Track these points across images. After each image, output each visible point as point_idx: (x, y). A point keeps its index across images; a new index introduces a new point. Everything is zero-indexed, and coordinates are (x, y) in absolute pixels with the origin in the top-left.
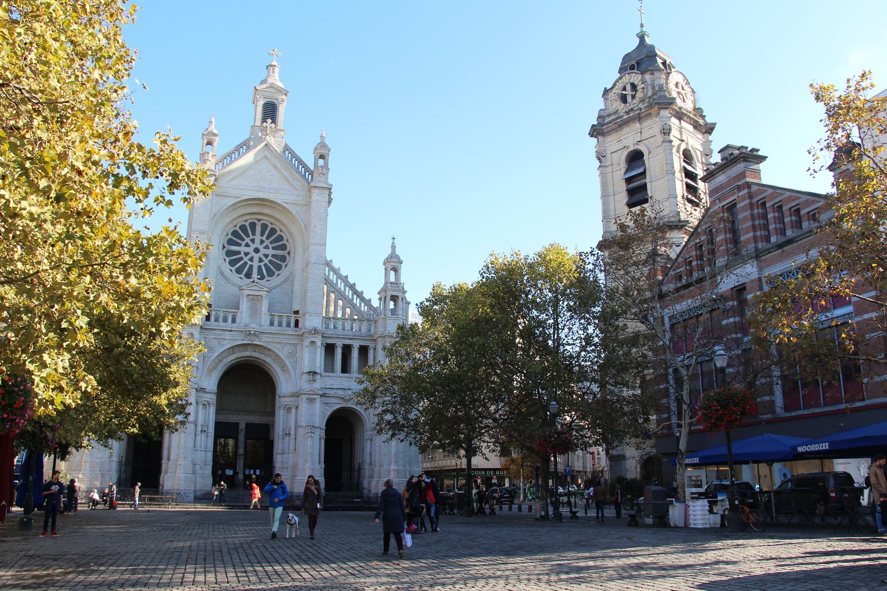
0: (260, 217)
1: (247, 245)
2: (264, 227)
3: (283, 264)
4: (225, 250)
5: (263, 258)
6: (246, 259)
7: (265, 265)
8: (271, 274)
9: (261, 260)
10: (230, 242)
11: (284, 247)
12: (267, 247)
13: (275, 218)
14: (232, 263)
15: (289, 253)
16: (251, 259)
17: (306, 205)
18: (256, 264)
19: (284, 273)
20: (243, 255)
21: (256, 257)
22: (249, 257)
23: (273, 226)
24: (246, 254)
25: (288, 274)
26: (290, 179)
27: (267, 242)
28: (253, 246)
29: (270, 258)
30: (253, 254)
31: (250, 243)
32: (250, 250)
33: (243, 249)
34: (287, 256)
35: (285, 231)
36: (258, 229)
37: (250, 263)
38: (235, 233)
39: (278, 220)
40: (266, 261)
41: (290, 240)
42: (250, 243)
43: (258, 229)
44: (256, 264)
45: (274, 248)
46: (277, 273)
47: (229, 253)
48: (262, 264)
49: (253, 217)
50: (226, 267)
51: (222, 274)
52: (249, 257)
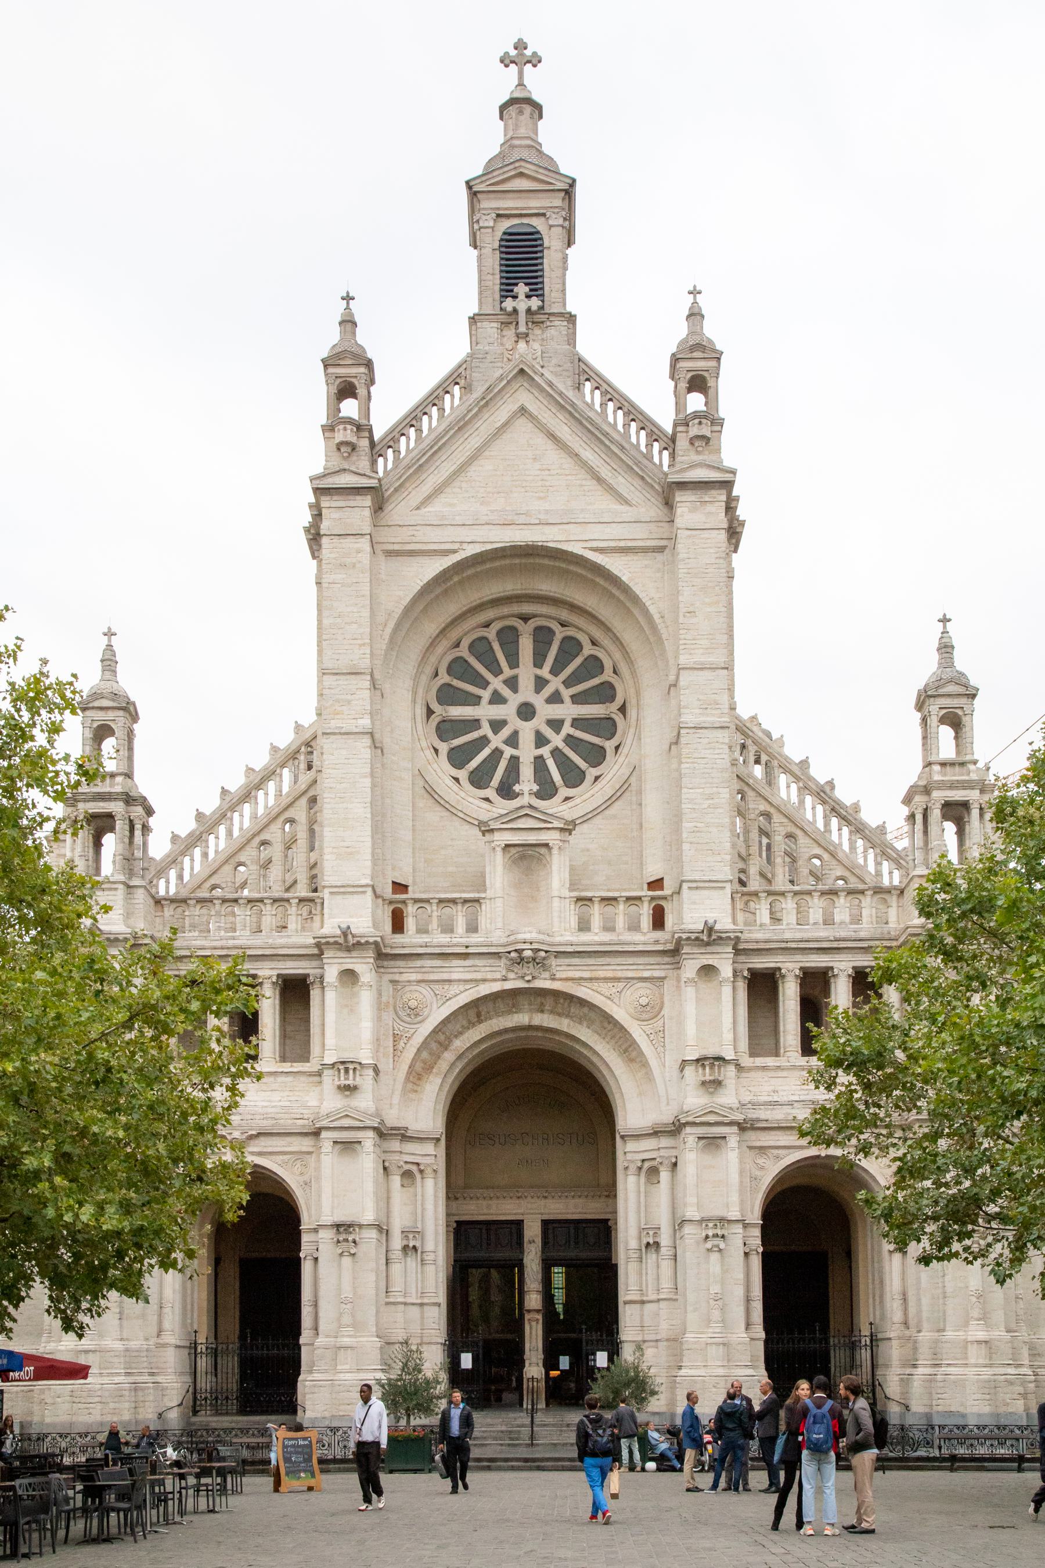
0: (527, 608)
1: (497, 699)
2: (542, 637)
3: (609, 745)
4: (435, 720)
5: (548, 732)
7: (556, 752)
8: (574, 777)
9: (541, 740)
10: (448, 695)
11: (606, 693)
12: (555, 698)
13: (573, 607)
14: (458, 758)
15: (623, 709)
16: (513, 740)
17: (661, 549)
19: (614, 770)
20: (486, 730)
21: (527, 730)
22: (506, 732)
23: (570, 632)
24: (497, 725)
25: (625, 771)
26: (605, 472)
27: (555, 683)
29: (567, 729)
30: (515, 723)
31: (506, 692)
32: (508, 711)
33: (485, 712)
34: (618, 718)
35: (606, 641)
36: (526, 646)
38: (458, 668)
40: (557, 740)
41: (623, 668)
42: (506, 692)
43: (526, 646)
44: (527, 752)
45: (576, 699)
47: (446, 729)
48: (545, 751)
49: (506, 610)
50: (441, 772)
51: (430, 792)
52: (506, 732)
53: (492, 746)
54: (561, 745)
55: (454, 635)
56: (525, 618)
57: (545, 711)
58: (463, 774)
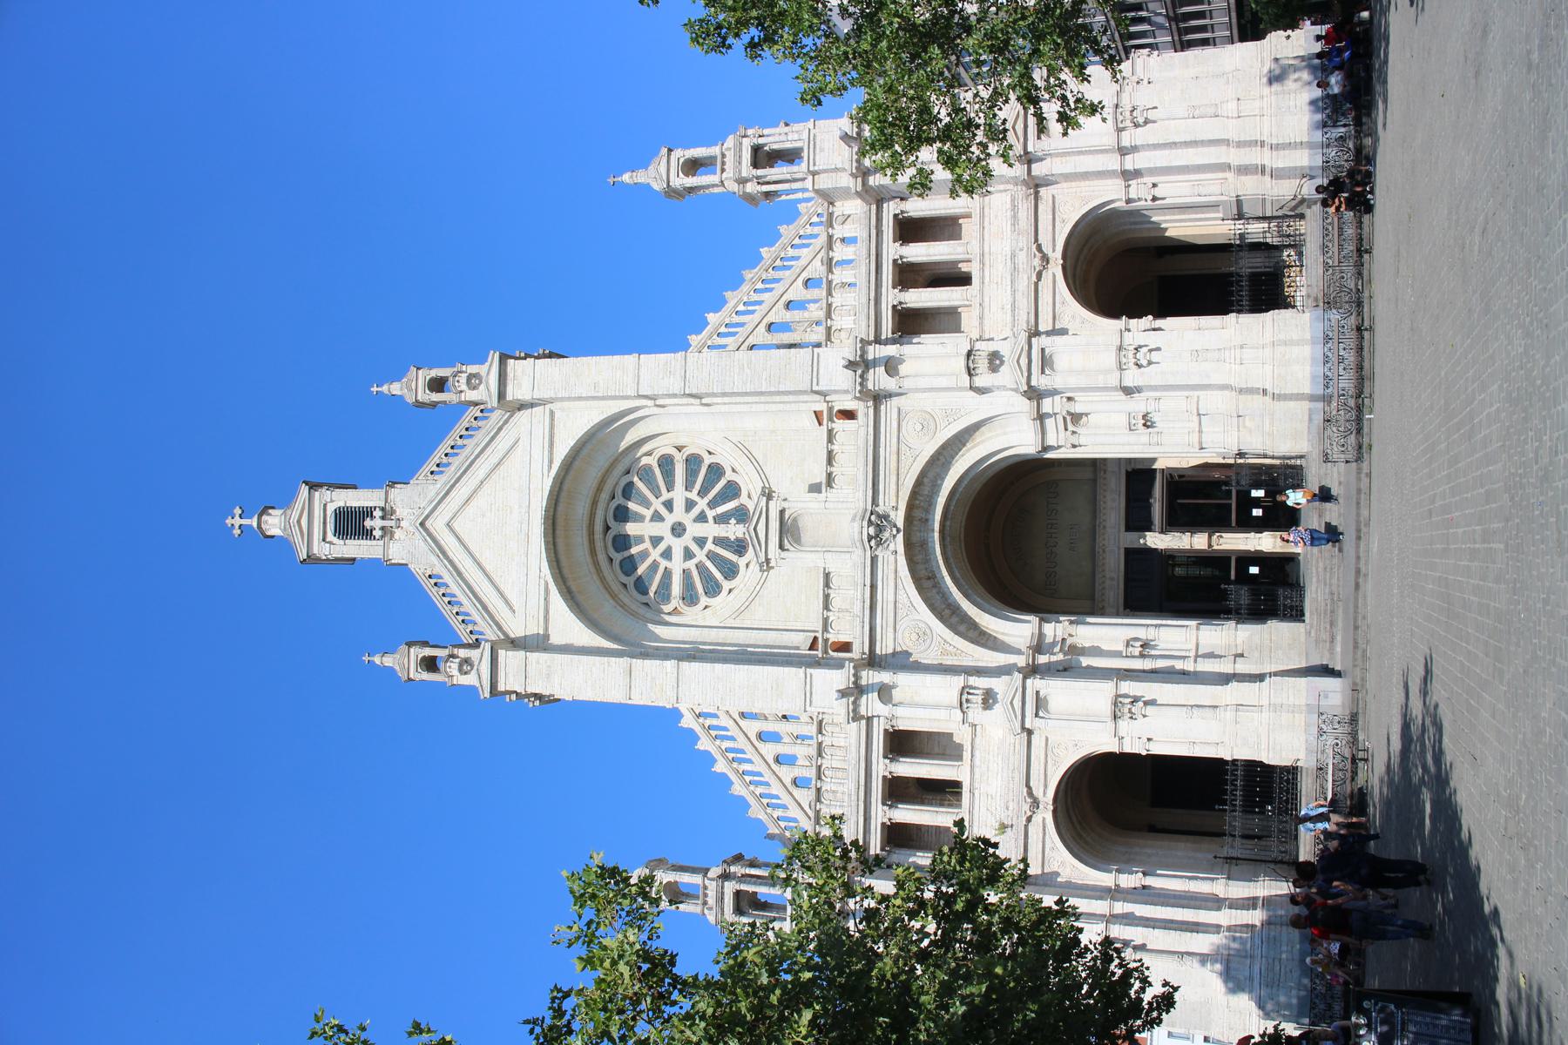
0: (599, 527)
3: (708, 460)
6: (701, 555)
7: (713, 504)
9: (702, 518)
13: (599, 489)
14: (713, 589)
15: (679, 449)
16: (701, 542)
18: (711, 530)
20: (691, 564)
22: (694, 548)
24: (688, 555)
28: (669, 540)
31: (662, 547)
37: (710, 546)
39: (602, 482)
42: (662, 547)
45: (670, 488)
46: (729, 475)
49: (599, 544)
52: (694, 548)
53: (704, 559)
54: (706, 500)
55: (616, 587)
56: (608, 528)
57: (679, 514)
58: (726, 585)
